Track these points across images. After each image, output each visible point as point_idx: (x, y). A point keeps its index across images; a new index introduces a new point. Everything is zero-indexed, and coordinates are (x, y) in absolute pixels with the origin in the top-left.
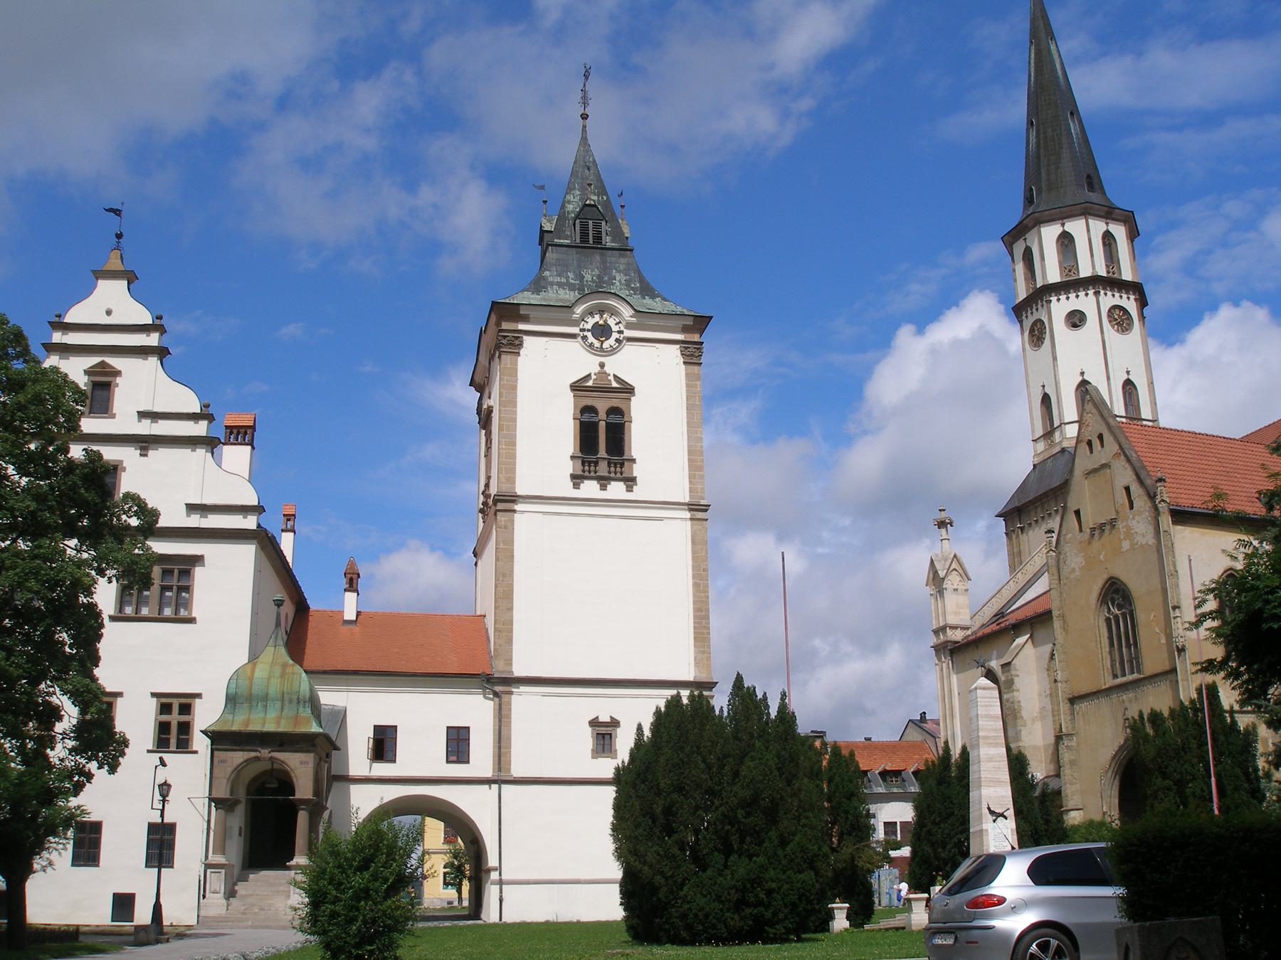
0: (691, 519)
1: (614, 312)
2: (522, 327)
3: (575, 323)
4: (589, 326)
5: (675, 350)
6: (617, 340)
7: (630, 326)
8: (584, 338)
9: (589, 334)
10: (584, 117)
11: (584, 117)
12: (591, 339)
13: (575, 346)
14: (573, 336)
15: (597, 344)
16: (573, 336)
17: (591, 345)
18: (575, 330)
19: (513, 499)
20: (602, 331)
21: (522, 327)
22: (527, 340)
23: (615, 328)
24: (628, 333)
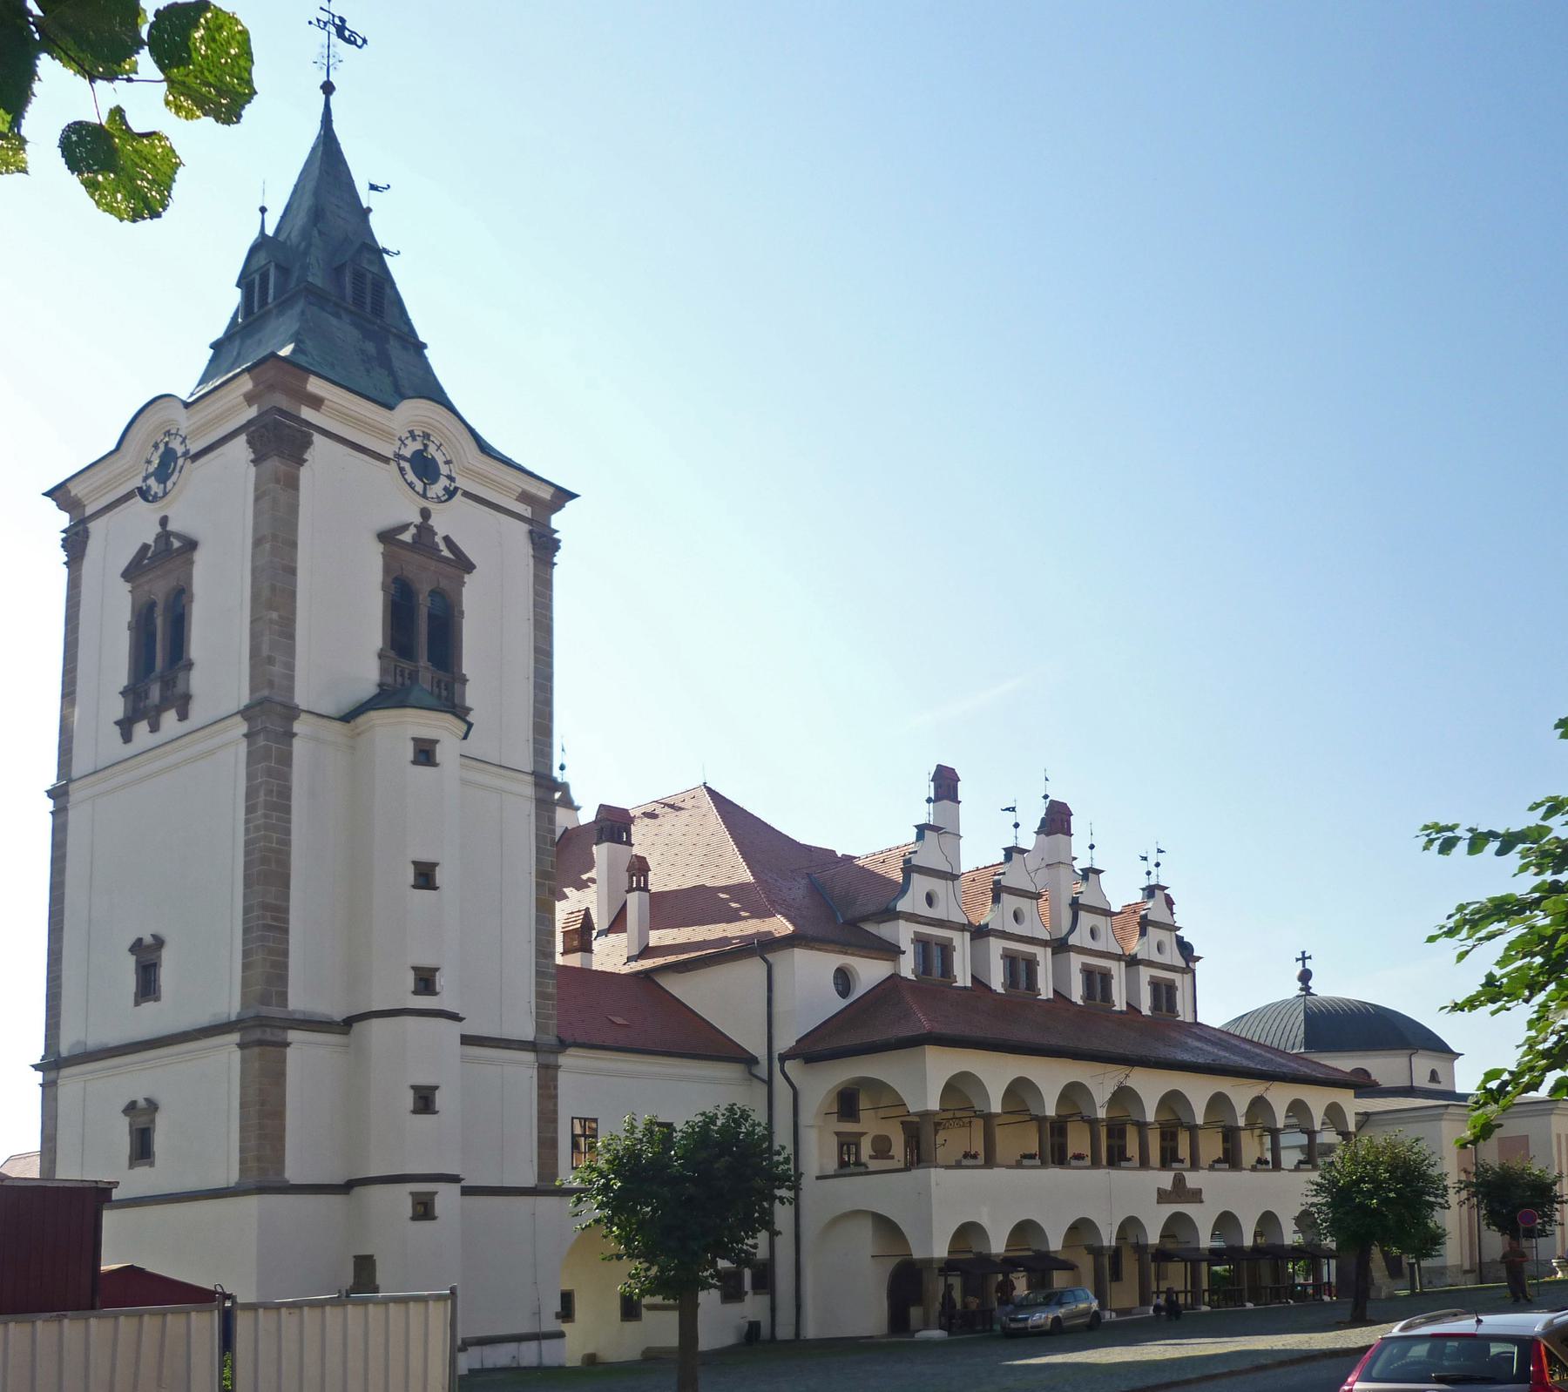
2: (307, 413)
3: (385, 434)
4: (407, 452)
5: (525, 527)
6: (446, 489)
8: (402, 470)
9: (406, 465)
12: (411, 476)
14: (386, 460)
15: (419, 486)
16: (386, 460)
17: (411, 485)
19: (292, 712)
20: (425, 467)
21: (307, 413)
22: (317, 438)
23: (444, 469)
24: (461, 483)
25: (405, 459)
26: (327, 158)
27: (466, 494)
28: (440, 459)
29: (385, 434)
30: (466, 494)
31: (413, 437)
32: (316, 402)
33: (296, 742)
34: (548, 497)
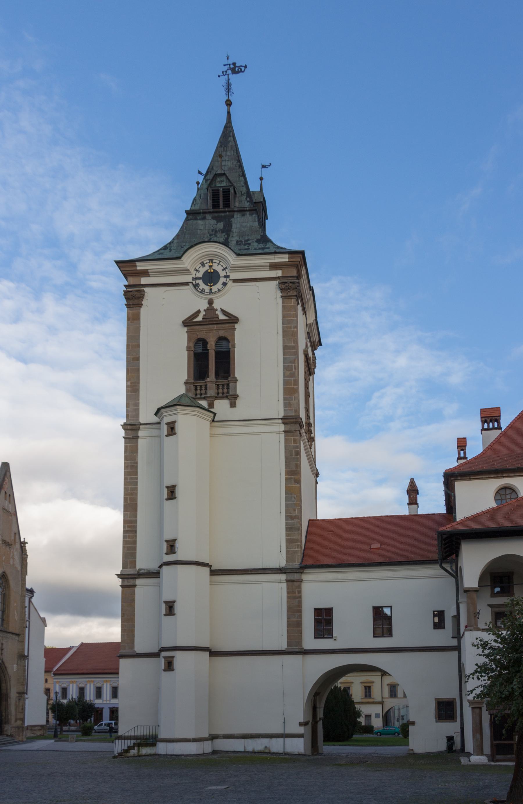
0: (285, 431)
1: (222, 259)
3: (186, 271)
4: (200, 275)
7: (236, 269)
9: (200, 282)
10: (229, 103)
11: (229, 103)
12: (202, 286)
13: (189, 291)
14: (187, 284)
16: (187, 284)
18: (188, 278)
24: (234, 276)
25: (200, 278)
26: (227, 139)
27: (235, 281)
28: (219, 269)
29: (186, 271)
30: (235, 281)
31: (203, 265)
32: (145, 273)
33: (140, 441)
34: (287, 260)
